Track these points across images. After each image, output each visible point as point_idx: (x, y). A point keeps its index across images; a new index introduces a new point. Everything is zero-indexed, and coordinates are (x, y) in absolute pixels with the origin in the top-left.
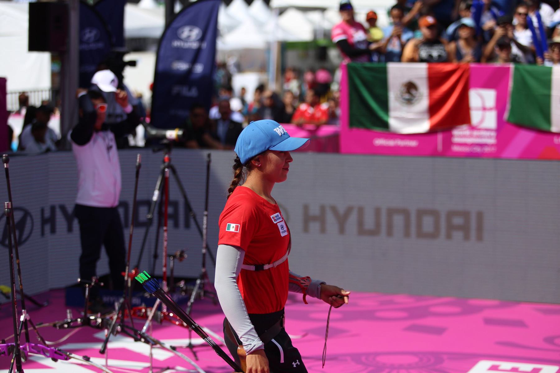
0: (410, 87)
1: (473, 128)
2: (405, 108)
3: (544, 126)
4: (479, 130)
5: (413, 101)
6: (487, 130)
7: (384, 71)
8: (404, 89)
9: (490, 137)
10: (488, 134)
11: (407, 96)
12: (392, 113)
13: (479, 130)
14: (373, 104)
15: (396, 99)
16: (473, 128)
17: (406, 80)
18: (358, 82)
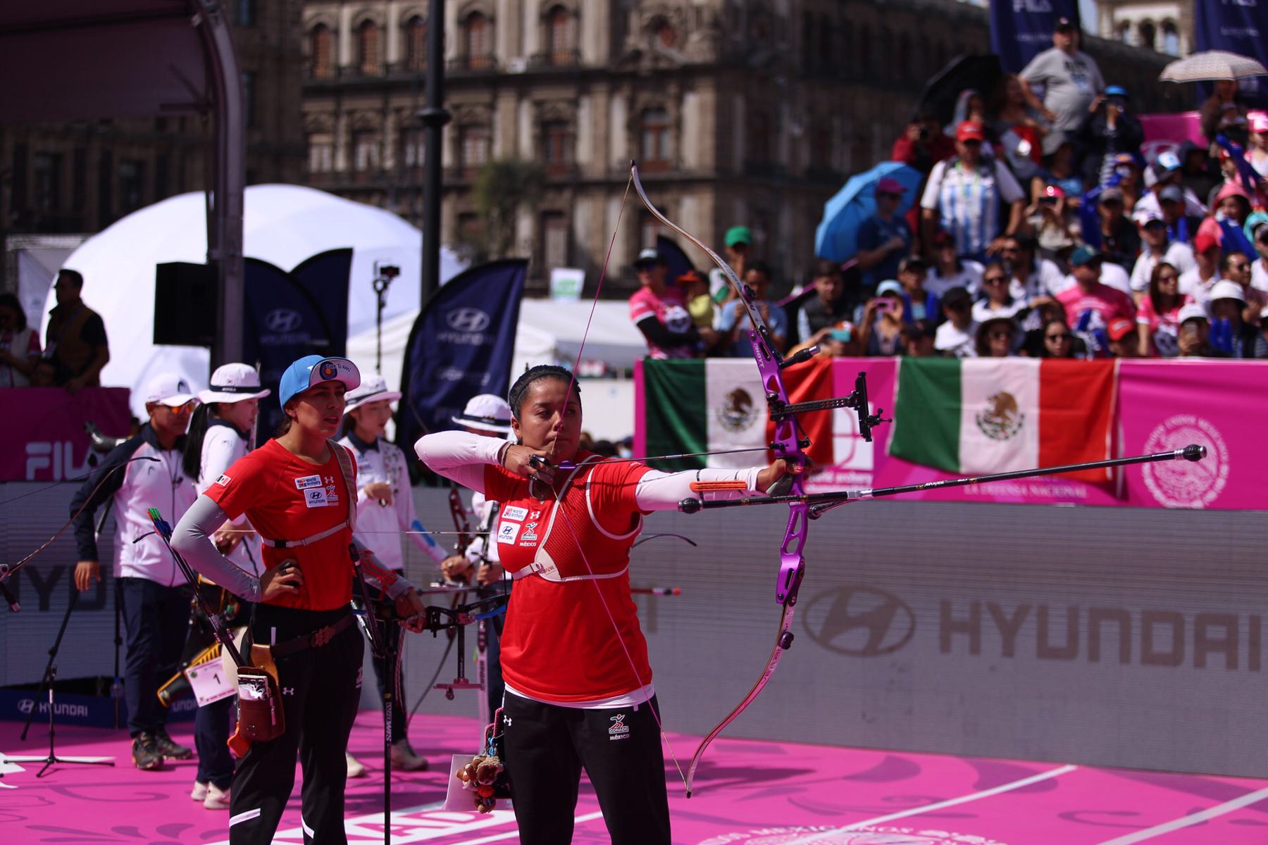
0: (740, 399)
1: (839, 470)
2: (731, 436)
3: (950, 465)
4: (847, 471)
5: (745, 424)
6: (859, 471)
7: (701, 372)
8: (731, 405)
9: (864, 484)
10: (860, 478)
11: (735, 415)
12: (712, 446)
13: (847, 471)
14: (682, 432)
15: (719, 419)
16: (839, 470)
17: (732, 387)
18: (659, 392)
